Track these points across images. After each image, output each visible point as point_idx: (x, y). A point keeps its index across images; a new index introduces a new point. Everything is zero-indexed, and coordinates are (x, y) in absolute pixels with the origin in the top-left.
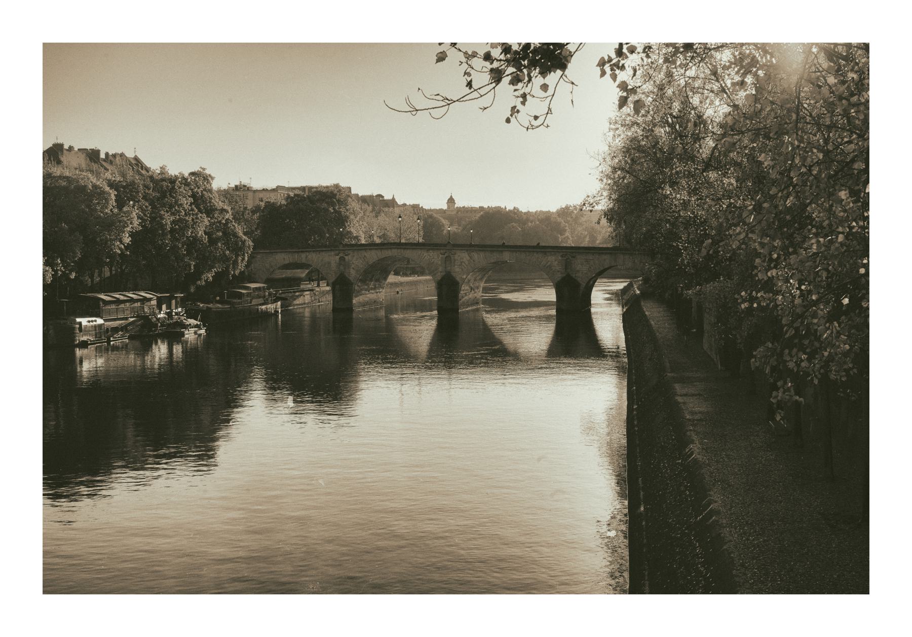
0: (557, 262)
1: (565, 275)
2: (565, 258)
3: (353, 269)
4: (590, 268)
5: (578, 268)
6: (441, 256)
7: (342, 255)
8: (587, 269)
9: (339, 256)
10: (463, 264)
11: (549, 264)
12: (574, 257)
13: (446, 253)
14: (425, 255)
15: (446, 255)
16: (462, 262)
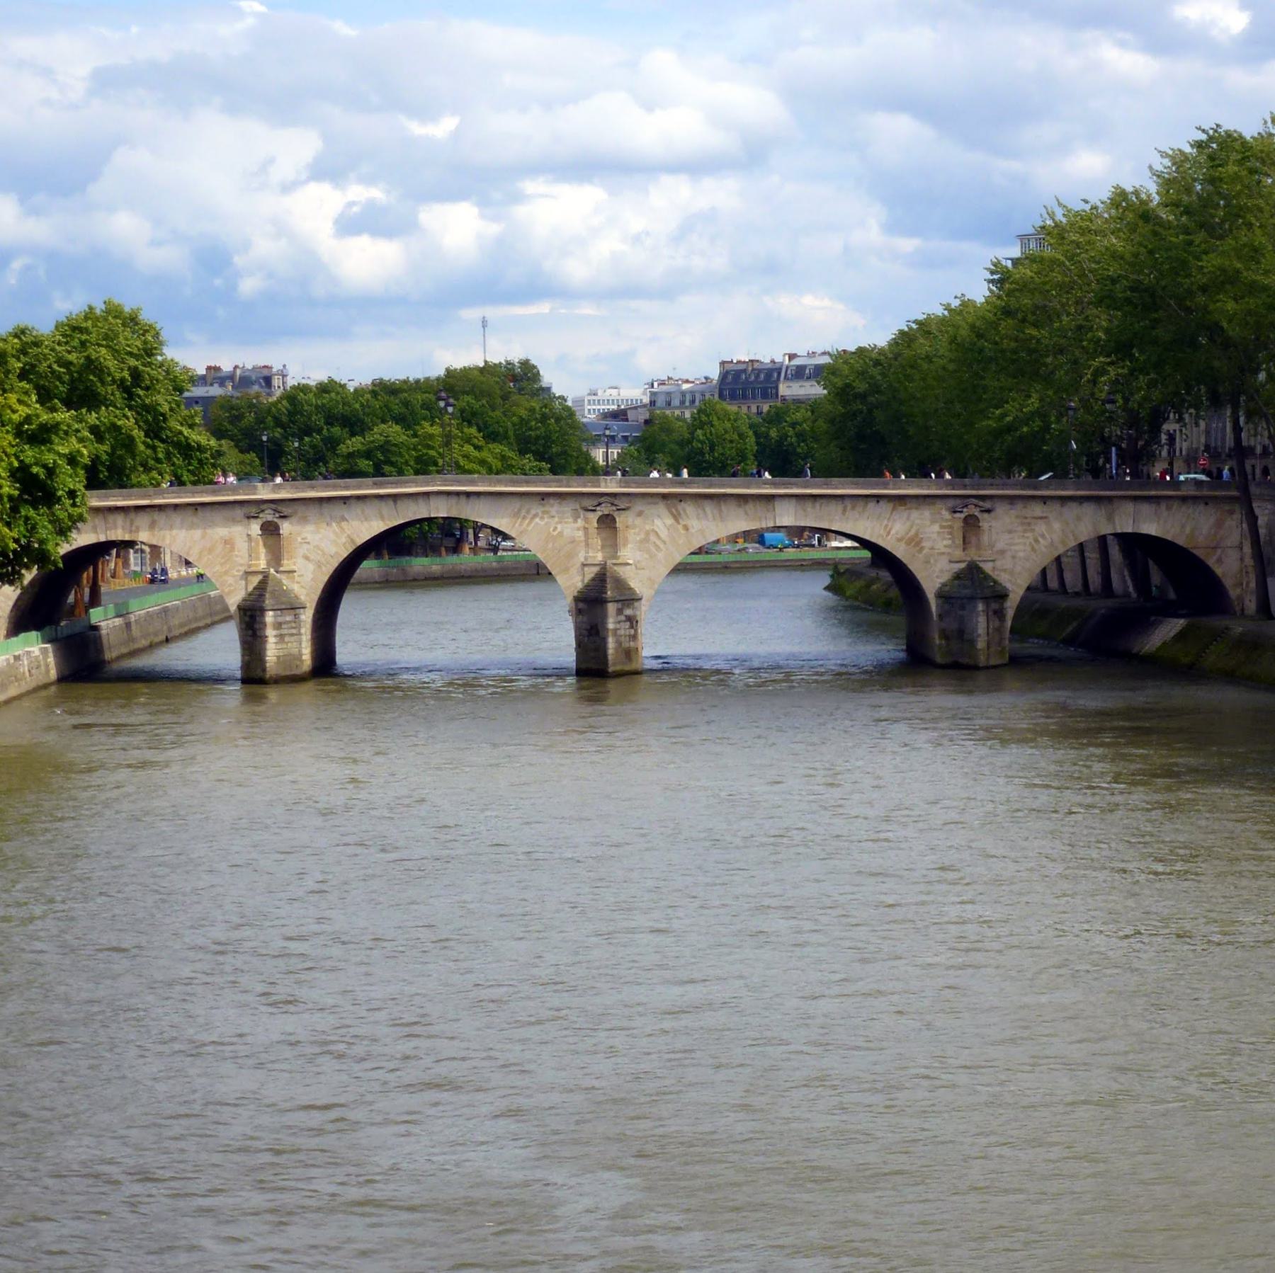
0: (936, 528)
1: (963, 565)
2: (962, 516)
3: (307, 558)
4: (1036, 541)
5: (1000, 545)
6: (582, 512)
7: (270, 518)
8: (1029, 549)
9: (260, 522)
10: (653, 538)
11: (913, 532)
12: (988, 511)
13: (599, 504)
14: (533, 512)
15: (605, 509)
16: (647, 533)
